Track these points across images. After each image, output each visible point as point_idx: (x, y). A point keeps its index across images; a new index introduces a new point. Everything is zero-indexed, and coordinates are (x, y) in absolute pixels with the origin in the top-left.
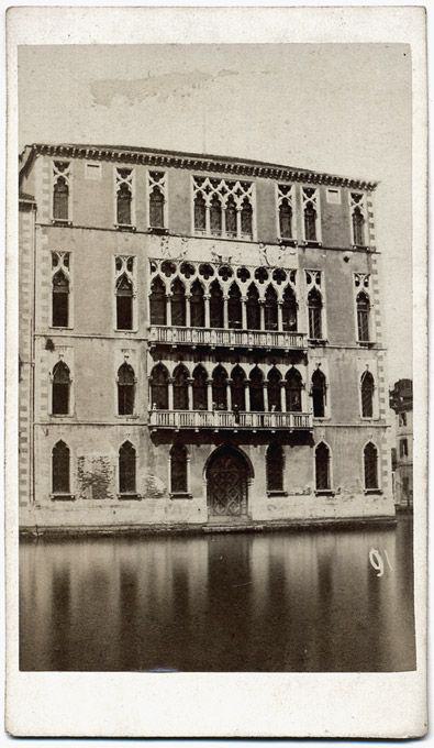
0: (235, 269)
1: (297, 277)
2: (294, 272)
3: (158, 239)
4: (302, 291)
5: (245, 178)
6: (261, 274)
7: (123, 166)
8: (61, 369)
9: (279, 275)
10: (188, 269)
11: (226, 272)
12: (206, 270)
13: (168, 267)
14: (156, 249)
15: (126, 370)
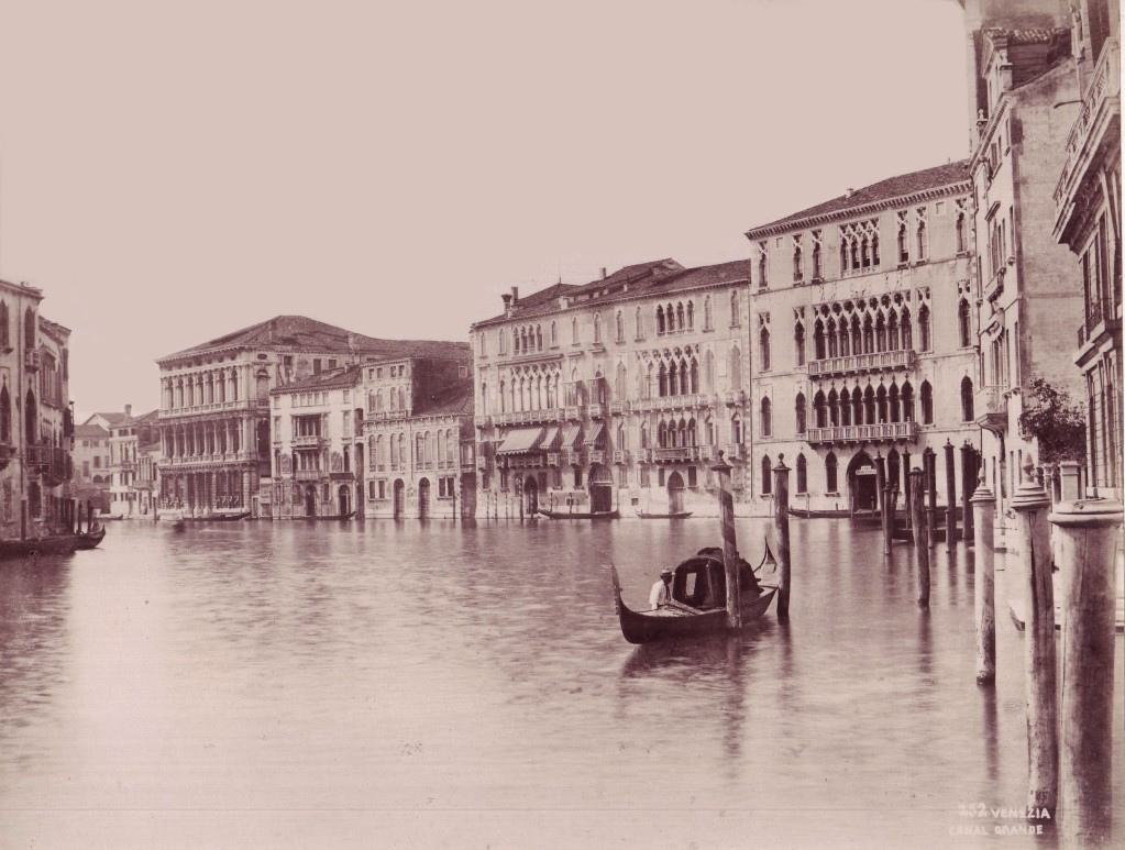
0: (867, 301)
1: (912, 295)
2: (908, 293)
3: (817, 287)
4: (914, 307)
5: (874, 216)
6: (886, 300)
7: (795, 233)
8: (766, 402)
9: (898, 298)
10: (837, 308)
11: (861, 305)
12: (849, 306)
13: (825, 310)
14: (816, 296)
15: (800, 399)
